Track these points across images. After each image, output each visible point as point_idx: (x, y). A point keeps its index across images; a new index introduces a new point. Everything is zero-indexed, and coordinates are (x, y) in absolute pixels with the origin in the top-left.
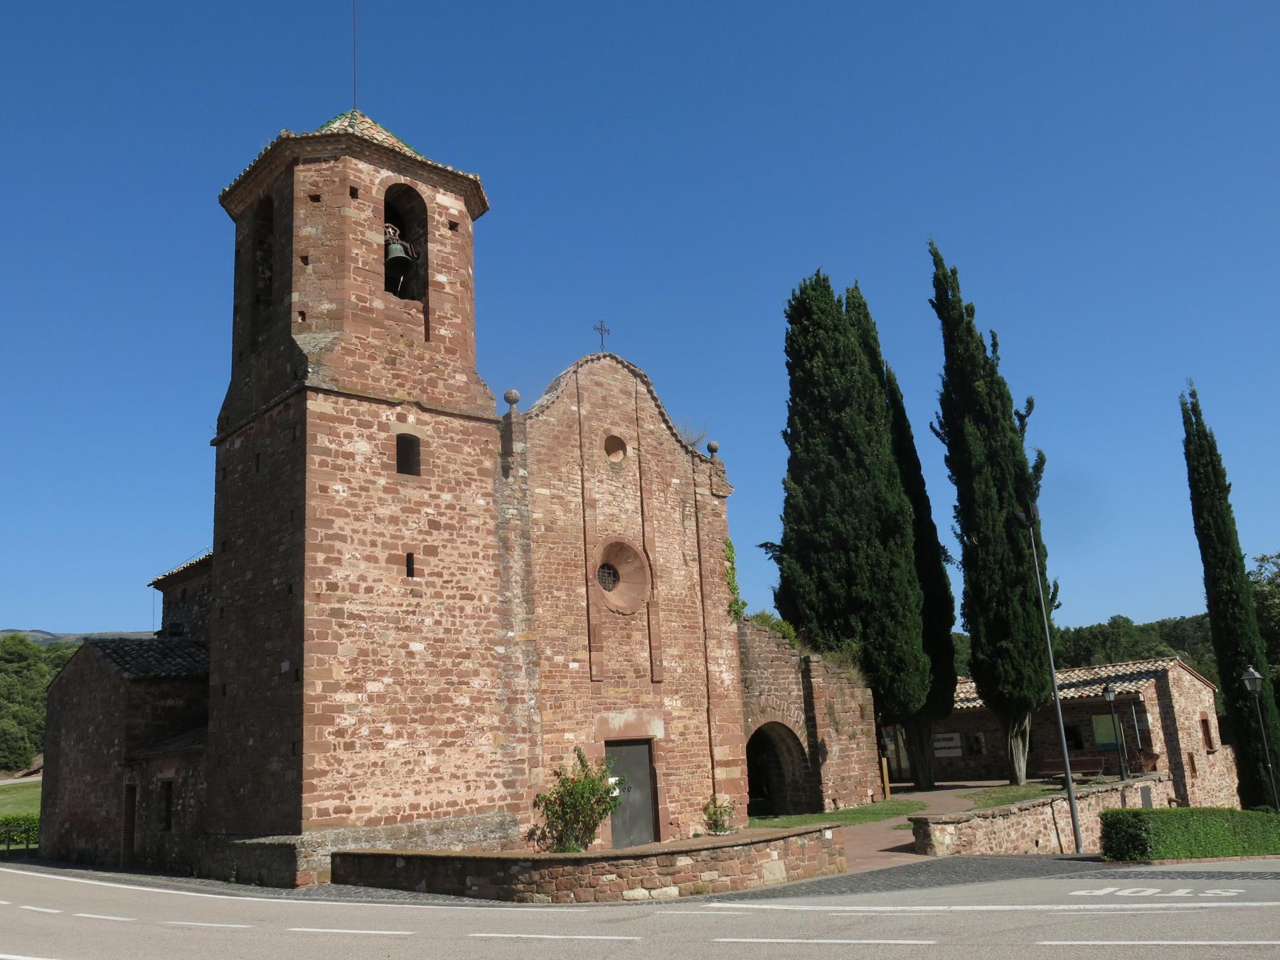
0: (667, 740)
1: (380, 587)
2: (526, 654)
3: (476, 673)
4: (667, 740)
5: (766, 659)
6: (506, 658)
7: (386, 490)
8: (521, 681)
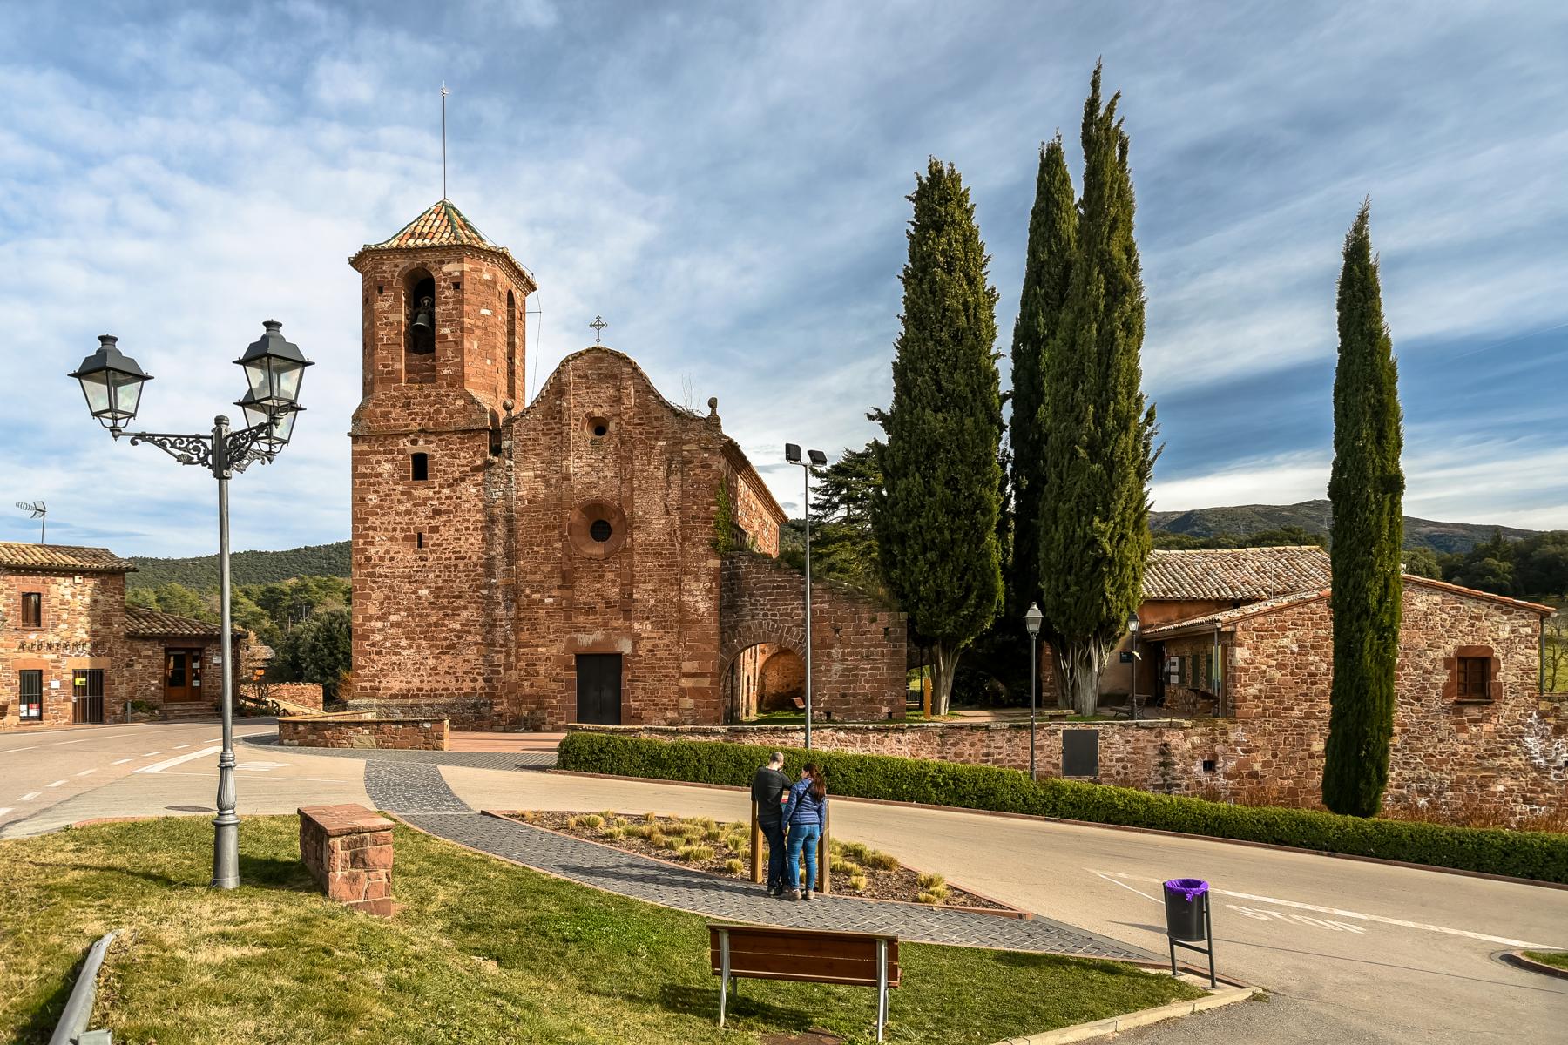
0: (635, 653)
1: (400, 556)
2: (505, 594)
3: (465, 608)
4: (635, 653)
5: (765, 588)
6: (489, 597)
7: (402, 493)
8: (500, 612)
